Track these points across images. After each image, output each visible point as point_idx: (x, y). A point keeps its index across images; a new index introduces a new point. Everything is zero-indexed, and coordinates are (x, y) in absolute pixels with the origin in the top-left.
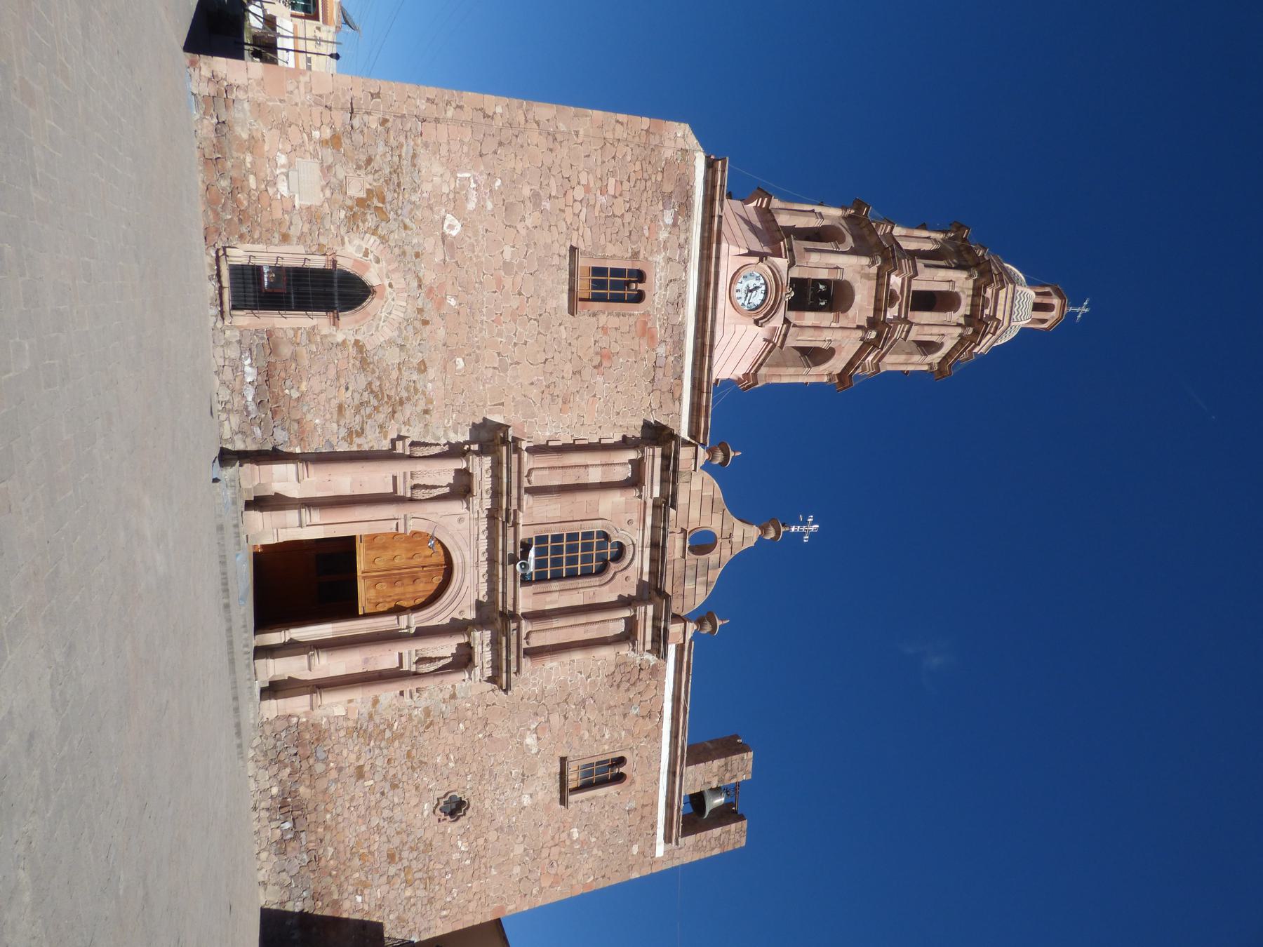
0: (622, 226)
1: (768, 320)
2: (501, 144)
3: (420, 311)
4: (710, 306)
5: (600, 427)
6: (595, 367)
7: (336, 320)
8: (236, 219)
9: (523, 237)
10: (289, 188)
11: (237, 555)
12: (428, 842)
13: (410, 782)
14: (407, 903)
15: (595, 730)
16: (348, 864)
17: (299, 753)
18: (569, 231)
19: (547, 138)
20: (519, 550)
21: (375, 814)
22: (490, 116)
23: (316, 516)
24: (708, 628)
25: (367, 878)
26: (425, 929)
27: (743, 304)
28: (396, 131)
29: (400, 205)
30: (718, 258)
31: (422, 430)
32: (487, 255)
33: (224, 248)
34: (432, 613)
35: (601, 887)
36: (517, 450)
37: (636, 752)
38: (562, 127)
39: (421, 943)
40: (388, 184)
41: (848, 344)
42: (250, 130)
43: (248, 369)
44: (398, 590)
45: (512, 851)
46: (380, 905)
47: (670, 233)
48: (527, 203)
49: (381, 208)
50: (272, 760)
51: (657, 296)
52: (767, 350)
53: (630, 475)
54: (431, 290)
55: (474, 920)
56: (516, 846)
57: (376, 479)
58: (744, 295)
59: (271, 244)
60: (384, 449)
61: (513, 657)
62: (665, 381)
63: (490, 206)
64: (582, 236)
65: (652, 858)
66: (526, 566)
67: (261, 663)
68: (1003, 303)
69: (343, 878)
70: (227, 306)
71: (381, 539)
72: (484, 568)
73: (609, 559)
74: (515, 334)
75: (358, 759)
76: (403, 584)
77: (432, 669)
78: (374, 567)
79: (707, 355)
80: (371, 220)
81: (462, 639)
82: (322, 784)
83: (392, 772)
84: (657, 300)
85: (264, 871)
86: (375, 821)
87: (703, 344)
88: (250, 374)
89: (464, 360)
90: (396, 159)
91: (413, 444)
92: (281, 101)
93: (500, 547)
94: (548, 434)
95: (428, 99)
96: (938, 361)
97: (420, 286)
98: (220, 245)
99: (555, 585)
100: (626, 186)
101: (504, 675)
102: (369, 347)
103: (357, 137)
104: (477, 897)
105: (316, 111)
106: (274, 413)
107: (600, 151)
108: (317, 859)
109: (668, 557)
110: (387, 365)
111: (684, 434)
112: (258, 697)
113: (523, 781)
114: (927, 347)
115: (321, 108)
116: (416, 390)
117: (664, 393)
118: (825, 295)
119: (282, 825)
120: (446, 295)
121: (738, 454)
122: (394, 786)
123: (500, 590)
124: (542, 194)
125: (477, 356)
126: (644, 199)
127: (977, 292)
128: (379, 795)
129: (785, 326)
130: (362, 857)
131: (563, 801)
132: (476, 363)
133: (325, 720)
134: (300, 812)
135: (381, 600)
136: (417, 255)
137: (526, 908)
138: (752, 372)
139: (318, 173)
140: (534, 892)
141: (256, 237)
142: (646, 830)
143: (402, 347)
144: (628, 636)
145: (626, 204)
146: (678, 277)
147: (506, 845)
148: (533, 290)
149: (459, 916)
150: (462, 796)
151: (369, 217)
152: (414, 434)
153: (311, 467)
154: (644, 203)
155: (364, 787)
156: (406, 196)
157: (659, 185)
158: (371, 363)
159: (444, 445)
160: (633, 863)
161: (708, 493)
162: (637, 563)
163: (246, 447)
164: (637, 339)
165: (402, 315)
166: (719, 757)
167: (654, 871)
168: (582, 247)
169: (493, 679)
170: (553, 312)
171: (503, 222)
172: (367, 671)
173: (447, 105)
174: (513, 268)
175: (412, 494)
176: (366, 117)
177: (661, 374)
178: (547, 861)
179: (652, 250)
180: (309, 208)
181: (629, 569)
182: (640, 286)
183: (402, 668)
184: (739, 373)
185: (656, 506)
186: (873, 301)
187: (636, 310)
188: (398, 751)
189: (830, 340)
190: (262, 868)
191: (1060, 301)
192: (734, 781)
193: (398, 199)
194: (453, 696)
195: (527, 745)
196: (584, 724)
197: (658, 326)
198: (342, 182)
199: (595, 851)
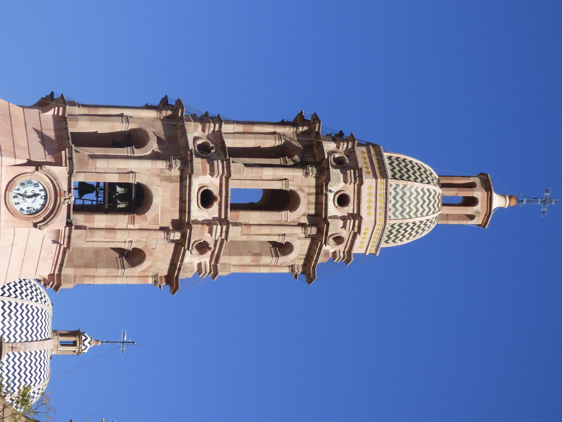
1: (47, 223)
96: (302, 263)
118: (123, 197)
189: (131, 242)
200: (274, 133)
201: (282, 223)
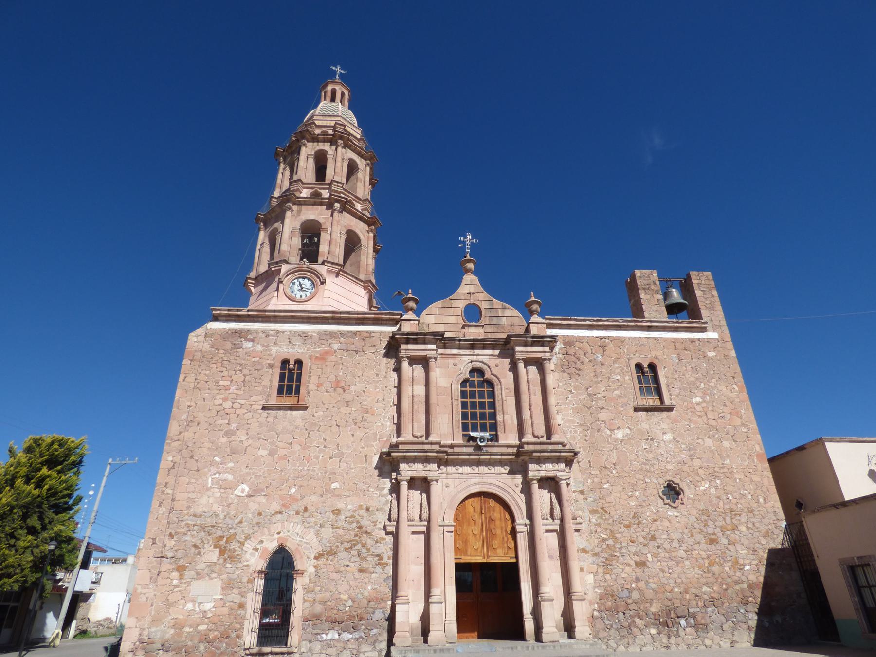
0: (251, 376)
1: (321, 275)
2: (192, 457)
3: (297, 513)
4: (307, 315)
5: (386, 387)
6: (344, 392)
7: (299, 572)
8: (226, 640)
9: (253, 442)
10: (209, 602)
11: (457, 651)
12: (701, 513)
13: (650, 525)
14: (752, 529)
15: (613, 386)
16: (717, 575)
17: (623, 610)
18: (251, 410)
19: (191, 427)
20: (471, 443)
21: (676, 553)
22: (174, 465)
23: (436, 591)
24: (536, 307)
25: (729, 561)
26: (775, 516)
27: (310, 293)
28: (178, 528)
29: (225, 525)
30: (275, 311)
31: (380, 513)
32: (263, 466)
33: (245, 649)
34: (516, 507)
35: (742, 379)
36: (396, 445)
37: (632, 356)
38: (185, 416)
39: (787, 520)
40: (212, 534)
41: (347, 221)
42: (169, 628)
43: (329, 637)
44: (499, 532)
45: (710, 447)
46: (753, 551)
47: (258, 343)
48: (231, 439)
49: (227, 539)
50: (628, 632)
51: (299, 351)
52: (345, 275)
53: (420, 366)
54: (284, 505)
55: (769, 477)
56: (706, 445)
57: (412, 546)
58: (305, 292)
59: (244, 616)
60: (392, 540)
61: (550, 447)
62: (357, 342)
63: (231, 465)
64: (256, 402)
65: (719, 341)
66: (482, 439)
67: (545, 637)
68: (326, 122)
69: (729, 580)
70: (284, 649)
71: (460, 543)
72: (484, 469)
73: (482, 379)
74: (318, 447)
75: (629, 565)
76: (494, 528)
77: (558, 508)
78: (481, 549)
79: (339, 315)
80: (234, 546)
81: (535, 486)
82: (649, 594)
83: (641, 539)
84: (302, 351)
85: (721, 643)
86: (681, 553)
87: (332, 318)
88: (333, 635)
89: (333, 483)
90: (196, 528)
91: (389, 520)
92: (152, 606)
93: (467, 457)
94: (389, 424)
95: (160, 506)
96: (364, 161)
97: (281, 513)
98: (243, 653)
99: (499, 417)
100: (225, 373)
101: (563, 454)
102: (320, 549)
103: (179, 554)
104: (748, 475)
105: (160, 581)
106: (361, 619)
107: (202, 392)
108: (712, 600)
109: (482, 336)
110: (333, 537)
111: (394, 329)
112: (572, 640)
113: (652, 440)
114: (352, 169)
115: (159, 578)
116: (352, 517)
117: (365, 344)
118: (311, 238)
119: (683, 626)
120: (288, 495)
121: (410, 291)
122: (653, 538)
123: (499, 457)
124: (226, 429)
125: (331, 473)
126: (235, 361)
127: (315, 139)
128: (660, 550)
129: (326, 264)
130: (711, 564)
131: (670, 409)
132: (336, 474)
133: (596, 590)
134: (672, 612)
135: (506, 545)
136: (260, 514)
137: (759, 437)
138: (362, 284)
139: (200, 582)
140: (745, 430)
141: (239, 627)
142: (695, 347)
143: (321, 526)
144: (539, 363)
145: (236, 373)
146: (287, 337)
147: (705, 452)
148: (289, 435)
149: (765, 489)
150: (662, 487)
151: (232, 547)
152: (383, 519)
153: (399, 594)
154: (237, 361)
155: (653, 561)
156: (220, 521)
157: (226, 351)
158: (331, 548)
159: (392, 497)
160: (723, 355)
161: (437, 311)
162: (485, 359)
163: (385, 640)
164: (327, 363)
165: (299, 525)
166: (638, 294)
167: (730, 339)
168: (262, 402)
169: (569, 463)
170: (305, 421)
171: (242, 456)
172: (559, 557)
173: (164, 493)
174: (273, 449)
175: (425, 521)
176: (167, 548)
177: (352, 346)
178: (719, 421)
179: (268, 355)
180: (223, 589)
181: (489, 364)
182: (292, 362)
183: (557, 530)
184: (362, 292)
185: (445, 347)
186: (315, 207)
187: (307, 364)
188: (624, 535)
190: (719, 644)
191: (330, 85)
192: (658, 283)
193: (221, 527)
194: (582, 492)
195: (623, 436)
196: (608, 394)
197: (320, 349)
198: (208, 566)
199: (712, 384)
200: (282, 173)
201: (334, 158)
